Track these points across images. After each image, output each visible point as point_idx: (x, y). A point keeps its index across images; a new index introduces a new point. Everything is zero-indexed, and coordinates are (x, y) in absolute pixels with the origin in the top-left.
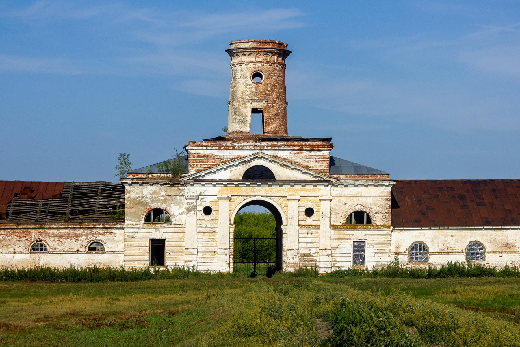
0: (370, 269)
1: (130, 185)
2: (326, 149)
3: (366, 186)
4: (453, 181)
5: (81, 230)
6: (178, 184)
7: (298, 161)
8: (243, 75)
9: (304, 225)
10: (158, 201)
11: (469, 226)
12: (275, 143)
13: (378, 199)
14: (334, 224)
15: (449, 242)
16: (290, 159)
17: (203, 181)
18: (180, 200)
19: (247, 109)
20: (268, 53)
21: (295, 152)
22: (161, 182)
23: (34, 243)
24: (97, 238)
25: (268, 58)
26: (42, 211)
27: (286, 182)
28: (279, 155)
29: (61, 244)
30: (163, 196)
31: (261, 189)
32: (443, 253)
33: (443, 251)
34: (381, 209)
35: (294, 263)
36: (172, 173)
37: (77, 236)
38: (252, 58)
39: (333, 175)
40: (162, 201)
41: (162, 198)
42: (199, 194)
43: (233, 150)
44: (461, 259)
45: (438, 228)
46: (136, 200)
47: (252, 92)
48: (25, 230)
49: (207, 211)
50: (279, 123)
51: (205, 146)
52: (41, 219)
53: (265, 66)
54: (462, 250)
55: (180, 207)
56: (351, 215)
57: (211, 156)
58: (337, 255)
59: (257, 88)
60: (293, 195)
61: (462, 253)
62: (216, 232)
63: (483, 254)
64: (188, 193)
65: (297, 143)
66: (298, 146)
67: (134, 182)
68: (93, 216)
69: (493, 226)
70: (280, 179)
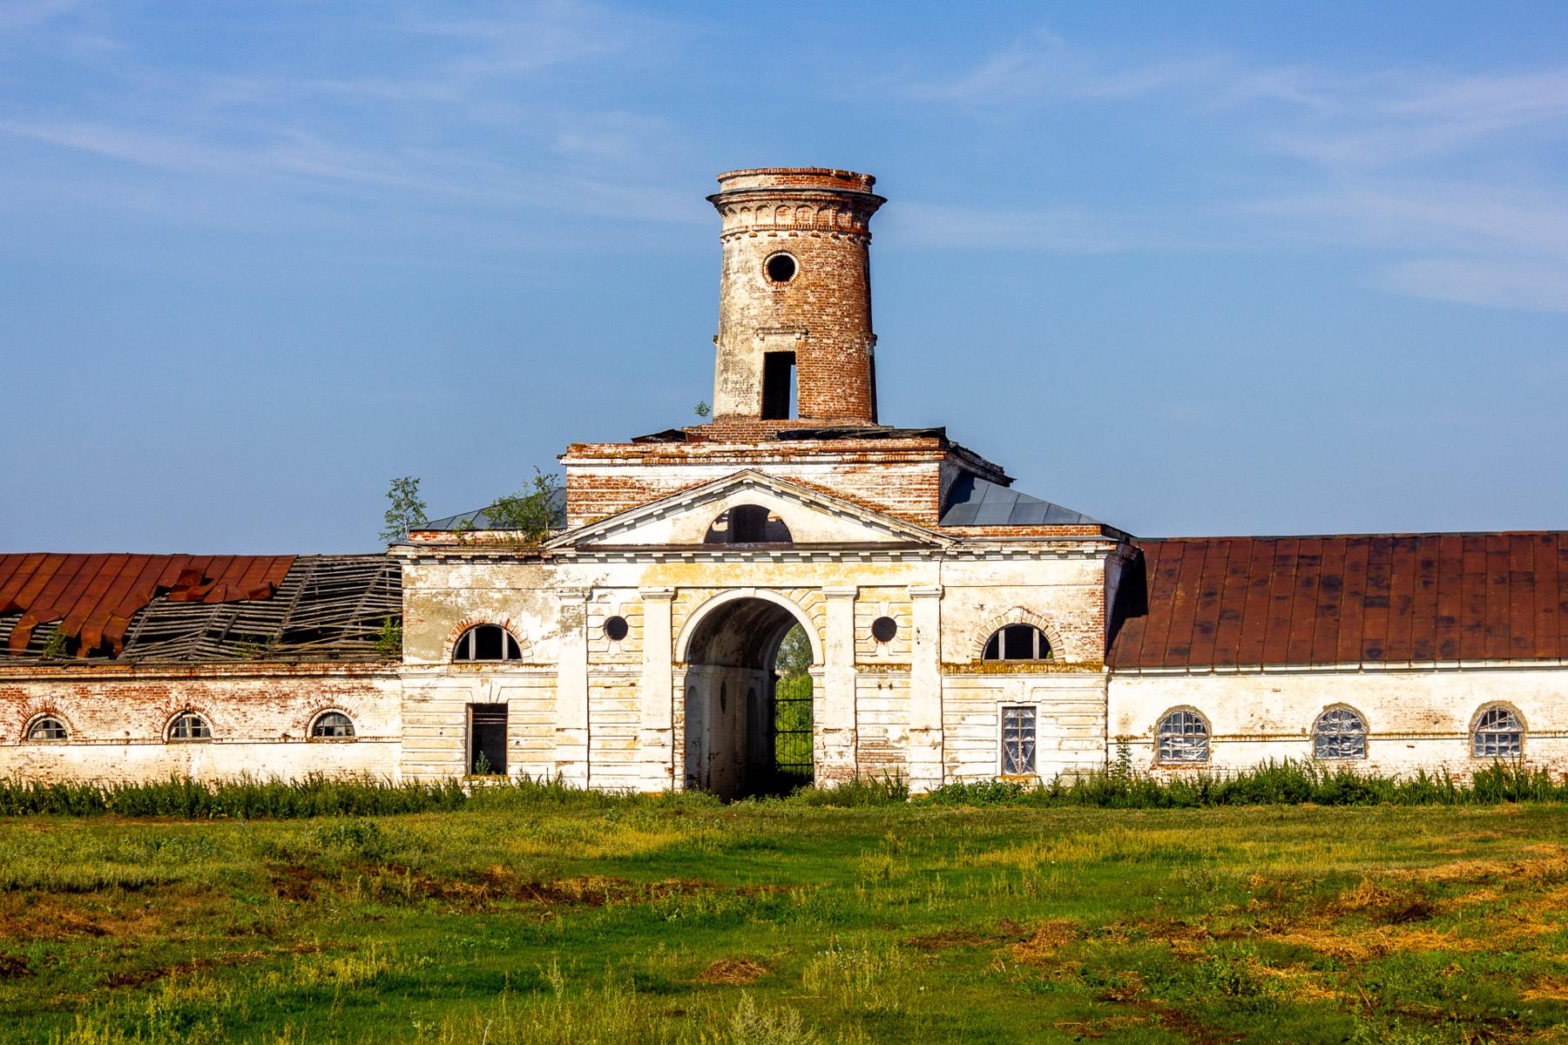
0: (1047, 781)
1: (416, 561)
2: (927, 457)
3: (1036, 557)
4: (1326, 540)
5: (294, 682)
6: (538, 558)
7: (855, 492)
8: (743, 264)
9: (870, 665)
10: (487, 603)
11: (1320, 664)
12: (793, 446)
13: (1070, 593)
14: (951, 661)
15: (1267, 706)
16: (834, 488)
17: (599, 549)
18: (545, 599)
19: (752, 355)
20: (809, 203)
21: (847, 467)
22: (493, 554)
23: (173, 718)
24: (335, 703)
25: (810, 215)
26: (211, 634)
27: (818, 550)
28: (805, 478)
29: (244, 719)
30: (500, 590)
31: (755, 569)
32: (1251, 736)
33: (1251, 733)
34: (1077, 619)
35: (842, 768)
36: (525, 529)
37: (286, 696)
38: (767, 217)
39: (947, 529)
40: (496, 605)
41: (498, 596)
42: (591, 584)
43: (681, 464)
44: (1299, 752)
45: (1235, 669)
46: (431, 601)
47: (767, 308)
48: (152, 683)
49: (616, 628)
50: (839, 390)
51: (608, 457)
52: (200, 653)
53: (800, 238)
54: (1304, 730)
55: (544, 619)
56: (995, 638)
57: (625, 483)
58: (957, 744)
59: (778, 297)
60: (840, 583)
61: (1301, 738)
62: (639, 684)
63: (1362, 739)
64: (563, 581)
65: (851, 444)
66: (853, 451)
67: (422, 554)
68: (332, 645)
69: (1386, 662)
70: (805, 540)
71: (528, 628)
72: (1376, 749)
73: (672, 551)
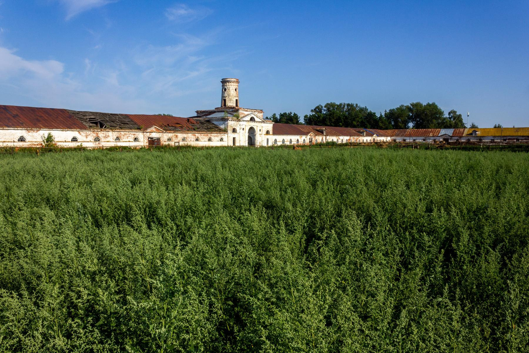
38: (234, 84)
71: (238, 129)
72: (285, 143)
73: (247, 121)
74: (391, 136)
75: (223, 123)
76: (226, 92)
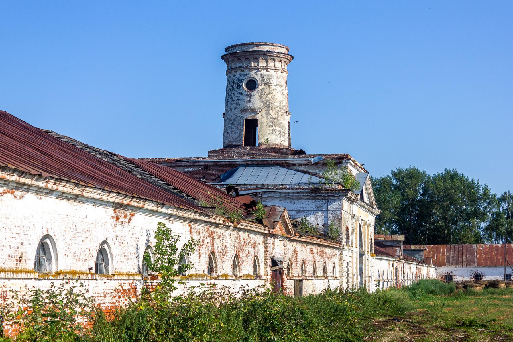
74: (438, 264)
75: (319, 208)
76: (256, 95)
